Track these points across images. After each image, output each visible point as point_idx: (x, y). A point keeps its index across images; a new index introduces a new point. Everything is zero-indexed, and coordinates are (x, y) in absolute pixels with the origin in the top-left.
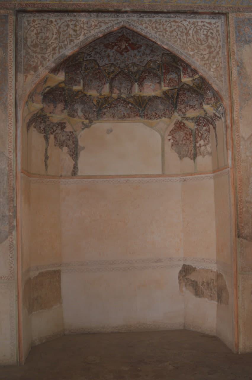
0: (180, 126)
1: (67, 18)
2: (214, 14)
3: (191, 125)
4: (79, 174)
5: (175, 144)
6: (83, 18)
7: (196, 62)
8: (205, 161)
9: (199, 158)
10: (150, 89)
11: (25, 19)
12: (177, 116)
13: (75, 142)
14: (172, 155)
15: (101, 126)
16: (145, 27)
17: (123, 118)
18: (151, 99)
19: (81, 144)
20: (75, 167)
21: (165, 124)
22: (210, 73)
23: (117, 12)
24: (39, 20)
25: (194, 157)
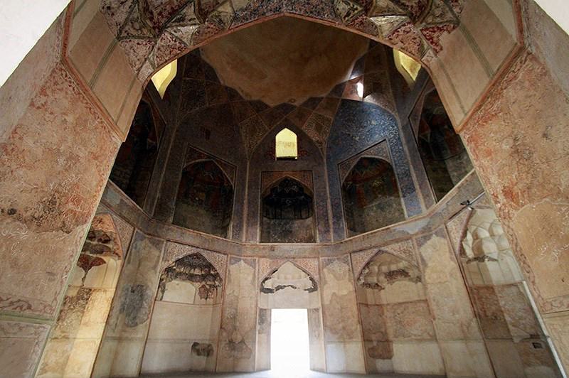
0: (203, 286)
1: (182, 246)
2: (224, 254)
3: (208, 287)
4: (163, 300)
5: (200, 293)
6: (187, 247)
7: (217, 268)
8: (210, 301)
9: (208, 299)
10: (197, 272)
11: (169, 243)
12: (204, 283)
13: (164, 287)
14: (198, 296)
15: (175, 282)
16: (205, 254)
17: (184, 280)
18: (196, 275)
19: (166, 288)
20: (162, 297)
21: (198, 285)
22: (220, 272)
23: (198, 247)
24: (173, 244)
25: (206, 299)
